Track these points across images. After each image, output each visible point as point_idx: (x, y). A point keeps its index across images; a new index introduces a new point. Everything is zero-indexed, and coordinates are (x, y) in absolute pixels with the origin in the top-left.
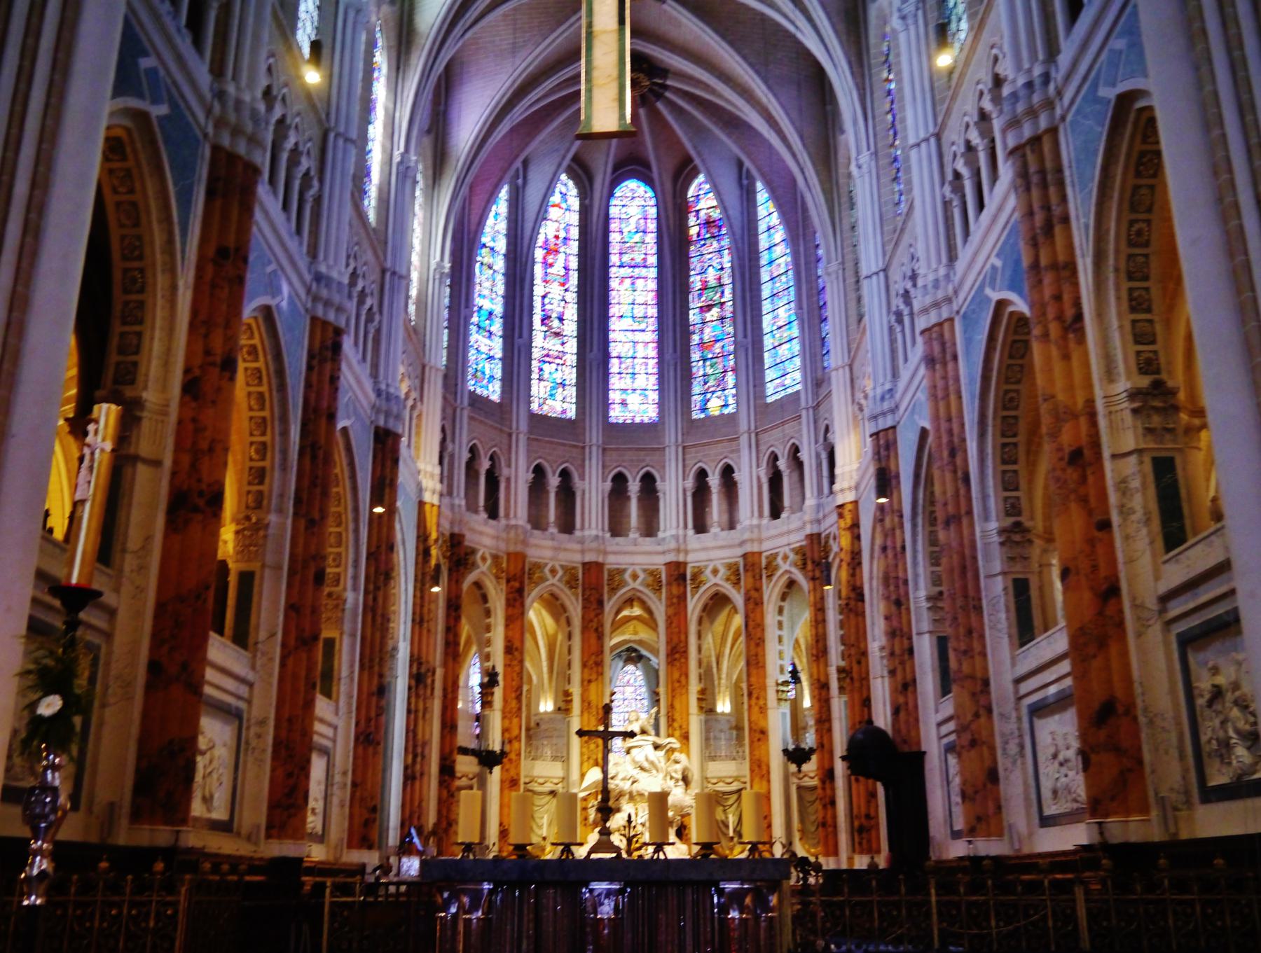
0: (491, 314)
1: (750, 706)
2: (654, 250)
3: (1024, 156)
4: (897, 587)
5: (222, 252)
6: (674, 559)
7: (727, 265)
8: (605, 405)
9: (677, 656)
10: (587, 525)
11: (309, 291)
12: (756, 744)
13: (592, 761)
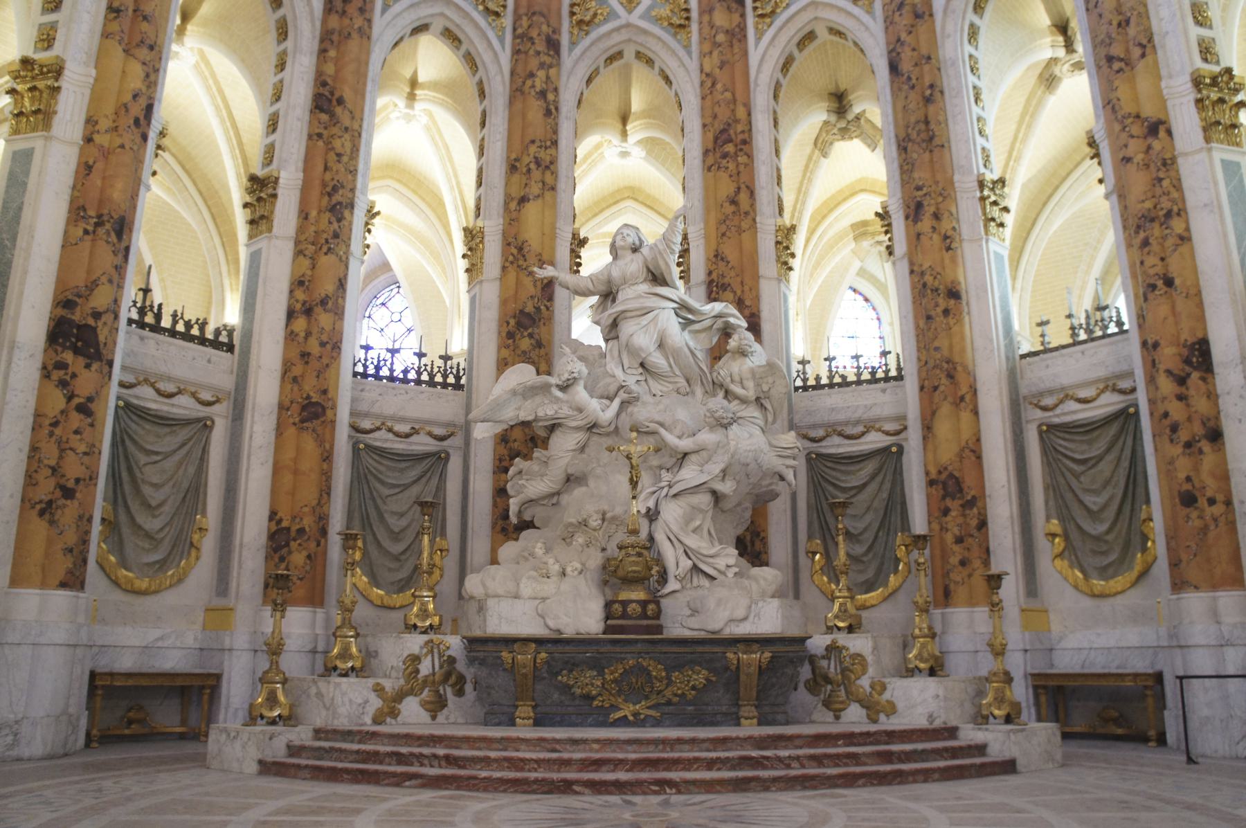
9: (730, 148)
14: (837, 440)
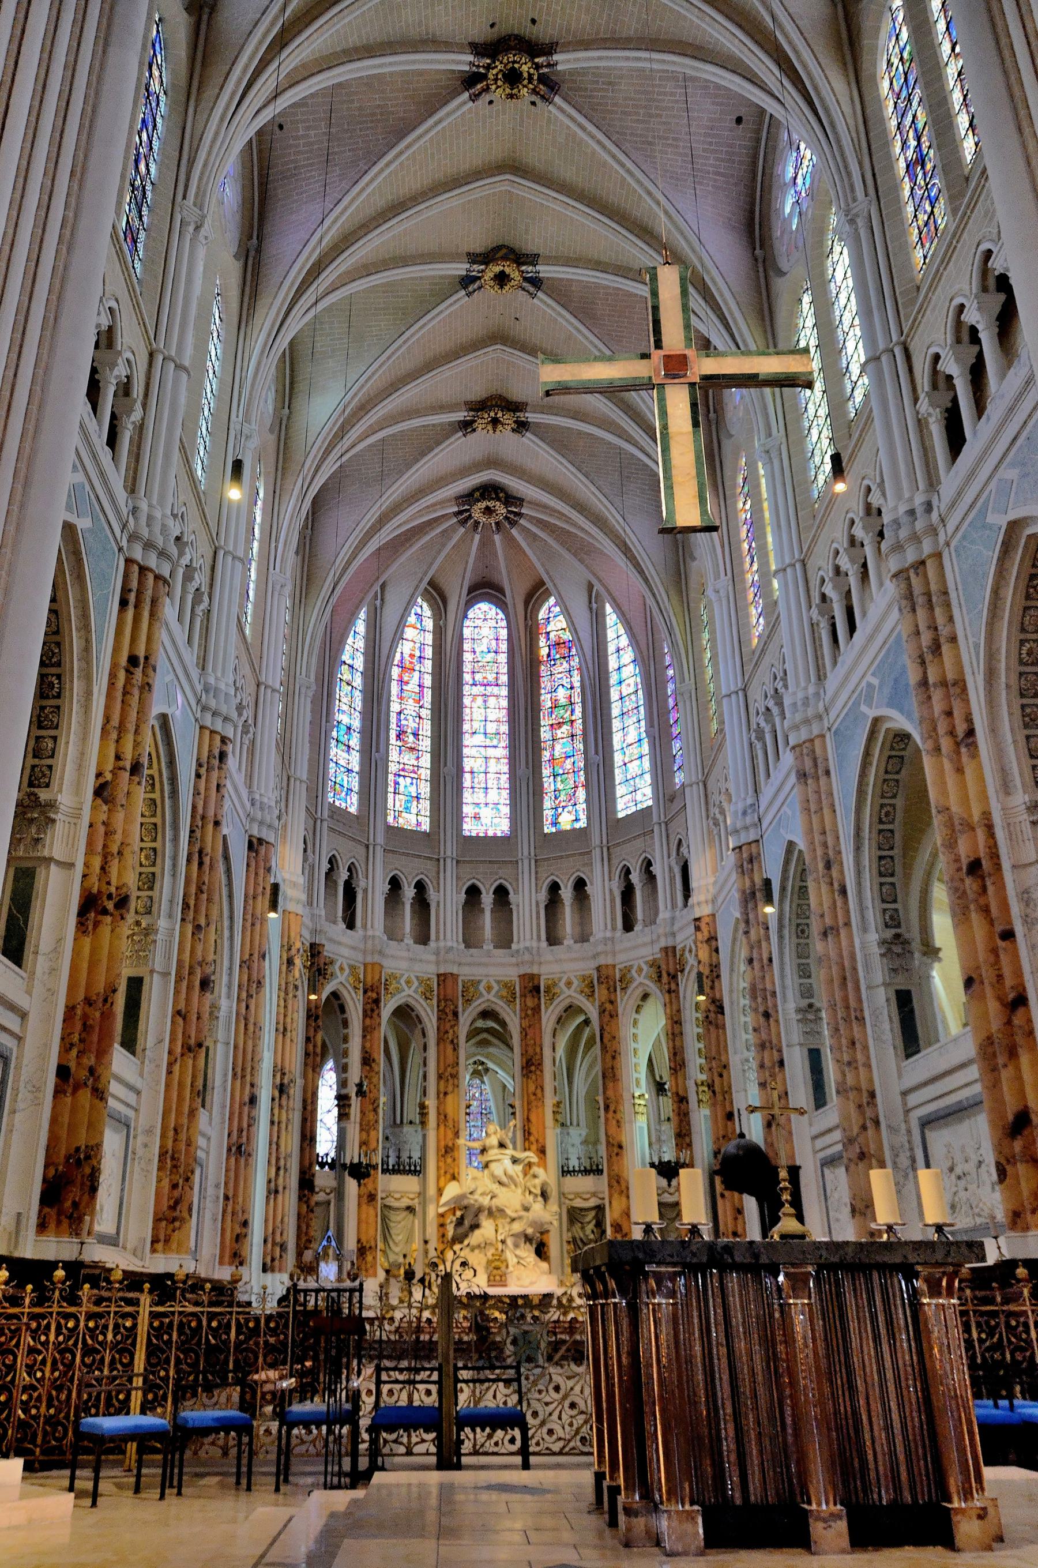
0: (349, 728)
1: (607, 1119)
2: (505, 670)
3: (908, 579)
4: (765, 999)
5: (133, 660)
6: (529, 971)
7: (577, 684)
8: (459, 818)
9: (533, 1068)
10: (442, 937)
11: (199, 701)
12: (614, 1158)
13: (448, 1176)
14: (579, 1200)
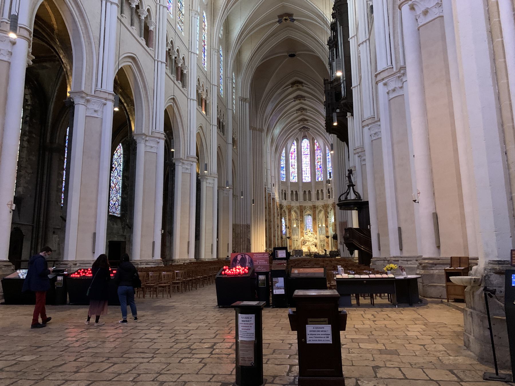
8: (302, 179)
